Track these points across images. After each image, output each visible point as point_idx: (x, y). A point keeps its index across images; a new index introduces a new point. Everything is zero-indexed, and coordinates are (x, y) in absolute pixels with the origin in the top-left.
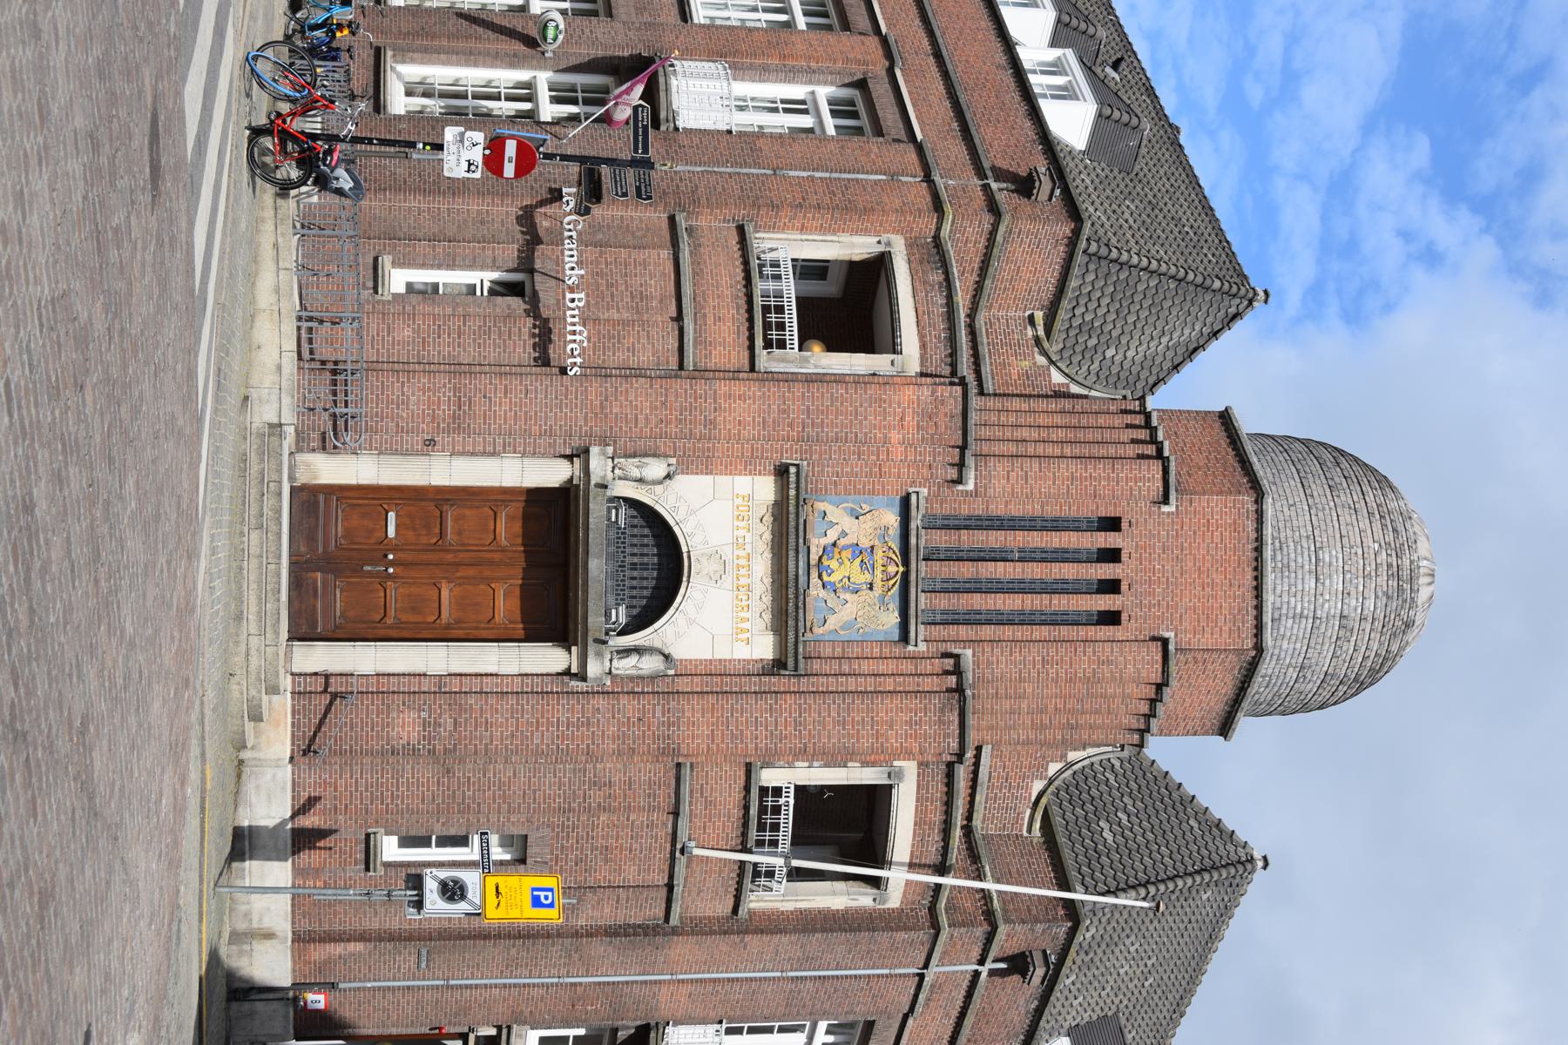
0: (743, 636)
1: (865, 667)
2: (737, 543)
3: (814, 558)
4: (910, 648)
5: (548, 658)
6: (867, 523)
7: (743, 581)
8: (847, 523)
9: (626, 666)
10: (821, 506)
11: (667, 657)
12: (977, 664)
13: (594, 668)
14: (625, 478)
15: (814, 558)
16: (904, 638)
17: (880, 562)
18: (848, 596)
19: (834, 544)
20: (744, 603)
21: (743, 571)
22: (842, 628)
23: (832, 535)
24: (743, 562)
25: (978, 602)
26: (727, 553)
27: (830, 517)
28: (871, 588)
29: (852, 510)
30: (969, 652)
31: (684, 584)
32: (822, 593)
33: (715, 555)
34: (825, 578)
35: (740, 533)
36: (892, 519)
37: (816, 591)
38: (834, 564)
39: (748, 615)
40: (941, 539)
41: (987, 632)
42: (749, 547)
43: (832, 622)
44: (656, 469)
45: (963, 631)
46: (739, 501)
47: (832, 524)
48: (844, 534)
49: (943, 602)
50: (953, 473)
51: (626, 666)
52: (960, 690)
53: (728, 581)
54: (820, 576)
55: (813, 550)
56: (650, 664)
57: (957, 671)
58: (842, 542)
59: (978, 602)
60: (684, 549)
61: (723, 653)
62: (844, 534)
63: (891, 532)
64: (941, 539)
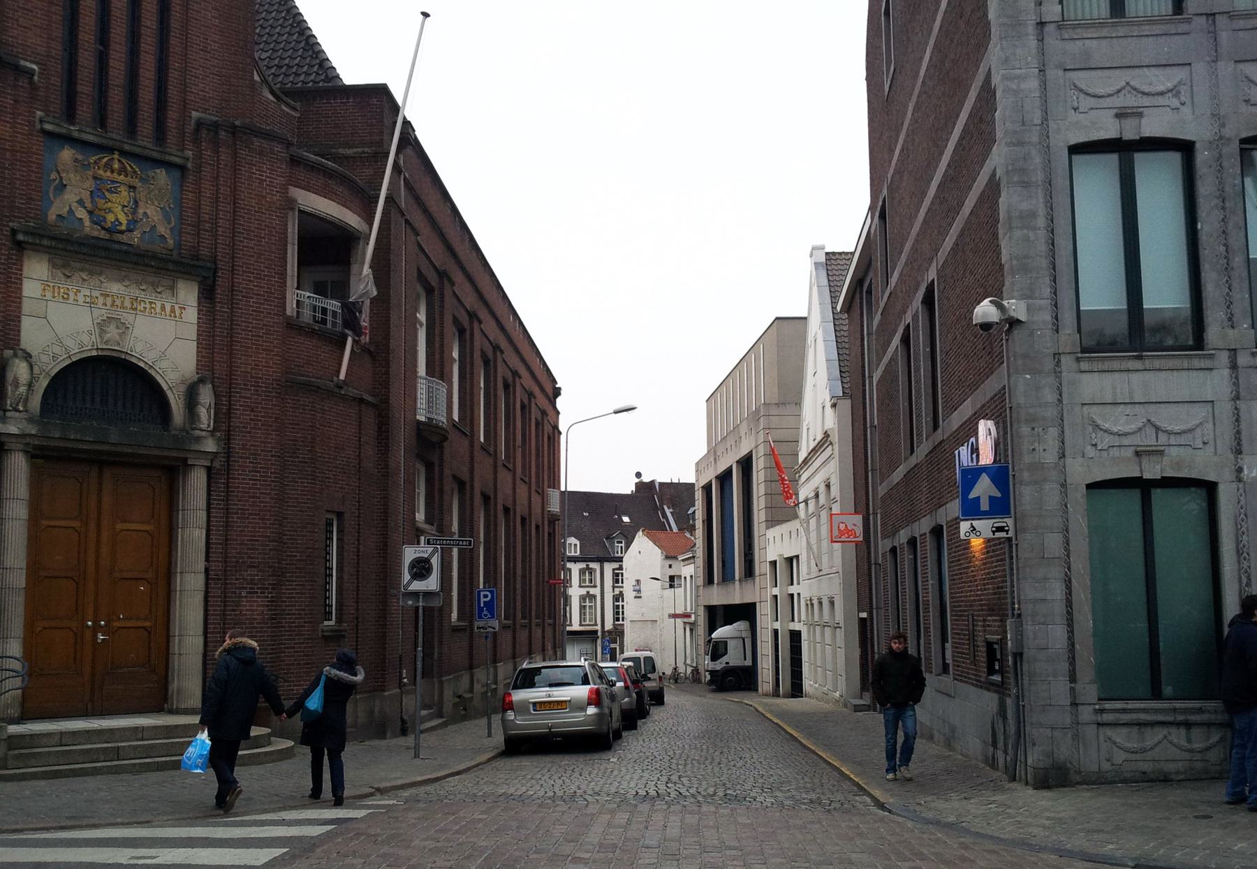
0: (178, 312)
1: (206, 208)
2: (91, 304)
3: (103, 235)
4: (189, 165)
5: (196, 484)
6: (71, 177)
7: (127, 304)
8: (70, 197)
9: (205, 416)
10: (52, 217)
11: (201, 381)
12: (205, 110)
13: (210, 446)
14: (27, 399)
15: (103, 235)
16: (182, 168)
17: (109, 174)
18: (141, 211)
19: (90, 213)
20: (148, 306)
21: (118, 302)
22: (169, 223)
23: (81, 213)
24: (109, 300)
25: (147, 95)
26: (101, 313)
27: (64, 211)
28: (134, 188)
29: (56, 189)
30: (195, 114)
31: (128, 358)
32: (137, 234)
33: (102, 327)
34: (124, 228)
35: (81, 299)
36: (67, 154)
37: (135, 238)
38: (111, 218)
39: (159, 304)
40: (85, 111)
41: (173, 92)
42: (96, 293)
43: (162, 229)
44: (20, 370)
45: (172, 114)
46: (49, 295)
47: (71, 211)
48: (81, 202)
49: (146, 126)
50: (23, 82)
51: (205, 416)
52: (234, 130)
53: (128, 317)
54: (122, 232)
55: (96, 234)
56: (206, 396)
57: (215, 127)
58: (88, 204)
59: (147, 95)
60: (94, 353)
61: (192, 332)
62: (81, 202)
63: (80, 157)
64: (85, 111)
